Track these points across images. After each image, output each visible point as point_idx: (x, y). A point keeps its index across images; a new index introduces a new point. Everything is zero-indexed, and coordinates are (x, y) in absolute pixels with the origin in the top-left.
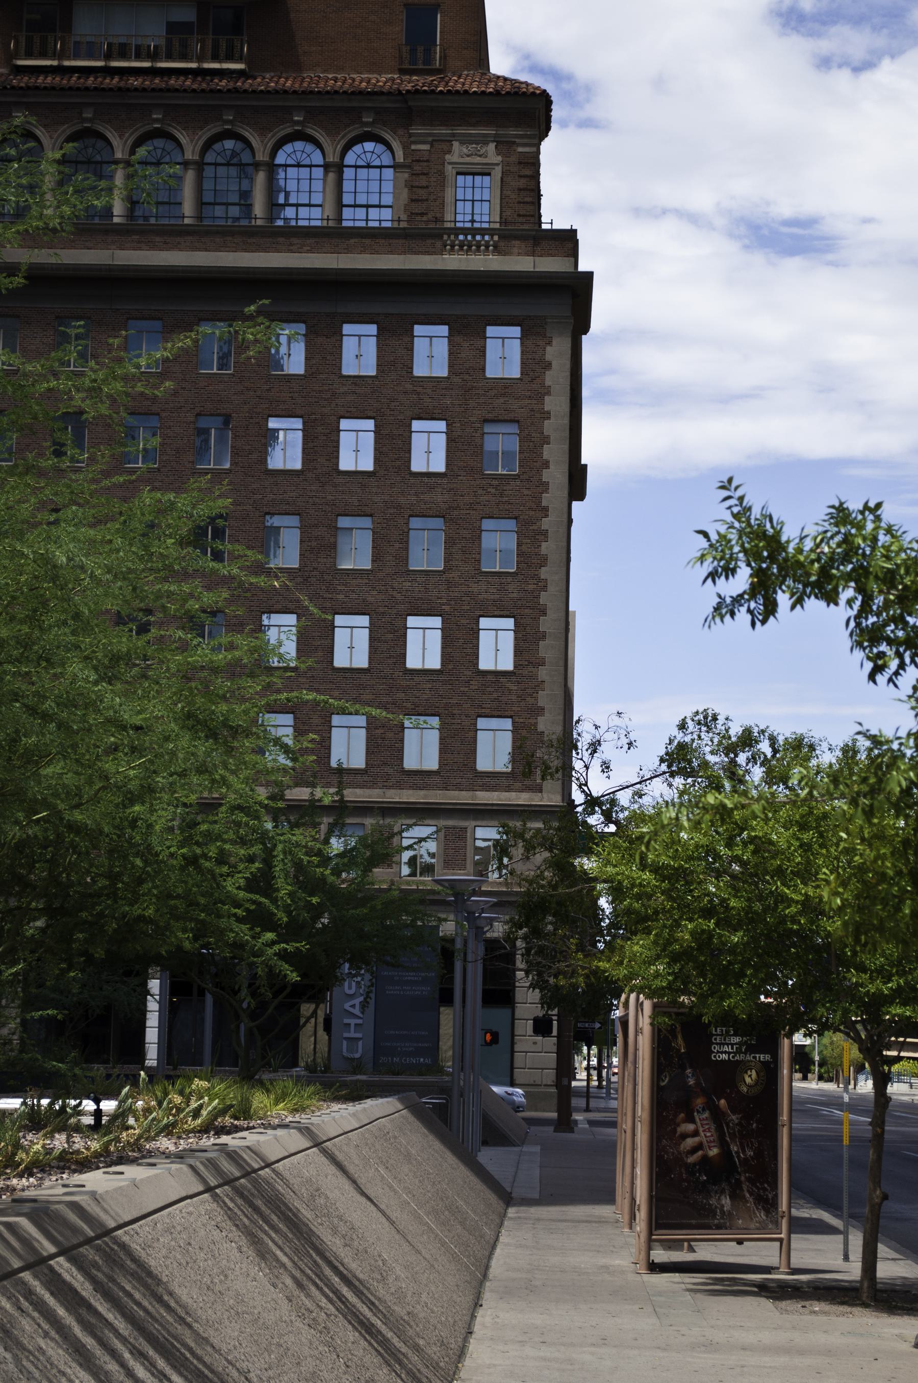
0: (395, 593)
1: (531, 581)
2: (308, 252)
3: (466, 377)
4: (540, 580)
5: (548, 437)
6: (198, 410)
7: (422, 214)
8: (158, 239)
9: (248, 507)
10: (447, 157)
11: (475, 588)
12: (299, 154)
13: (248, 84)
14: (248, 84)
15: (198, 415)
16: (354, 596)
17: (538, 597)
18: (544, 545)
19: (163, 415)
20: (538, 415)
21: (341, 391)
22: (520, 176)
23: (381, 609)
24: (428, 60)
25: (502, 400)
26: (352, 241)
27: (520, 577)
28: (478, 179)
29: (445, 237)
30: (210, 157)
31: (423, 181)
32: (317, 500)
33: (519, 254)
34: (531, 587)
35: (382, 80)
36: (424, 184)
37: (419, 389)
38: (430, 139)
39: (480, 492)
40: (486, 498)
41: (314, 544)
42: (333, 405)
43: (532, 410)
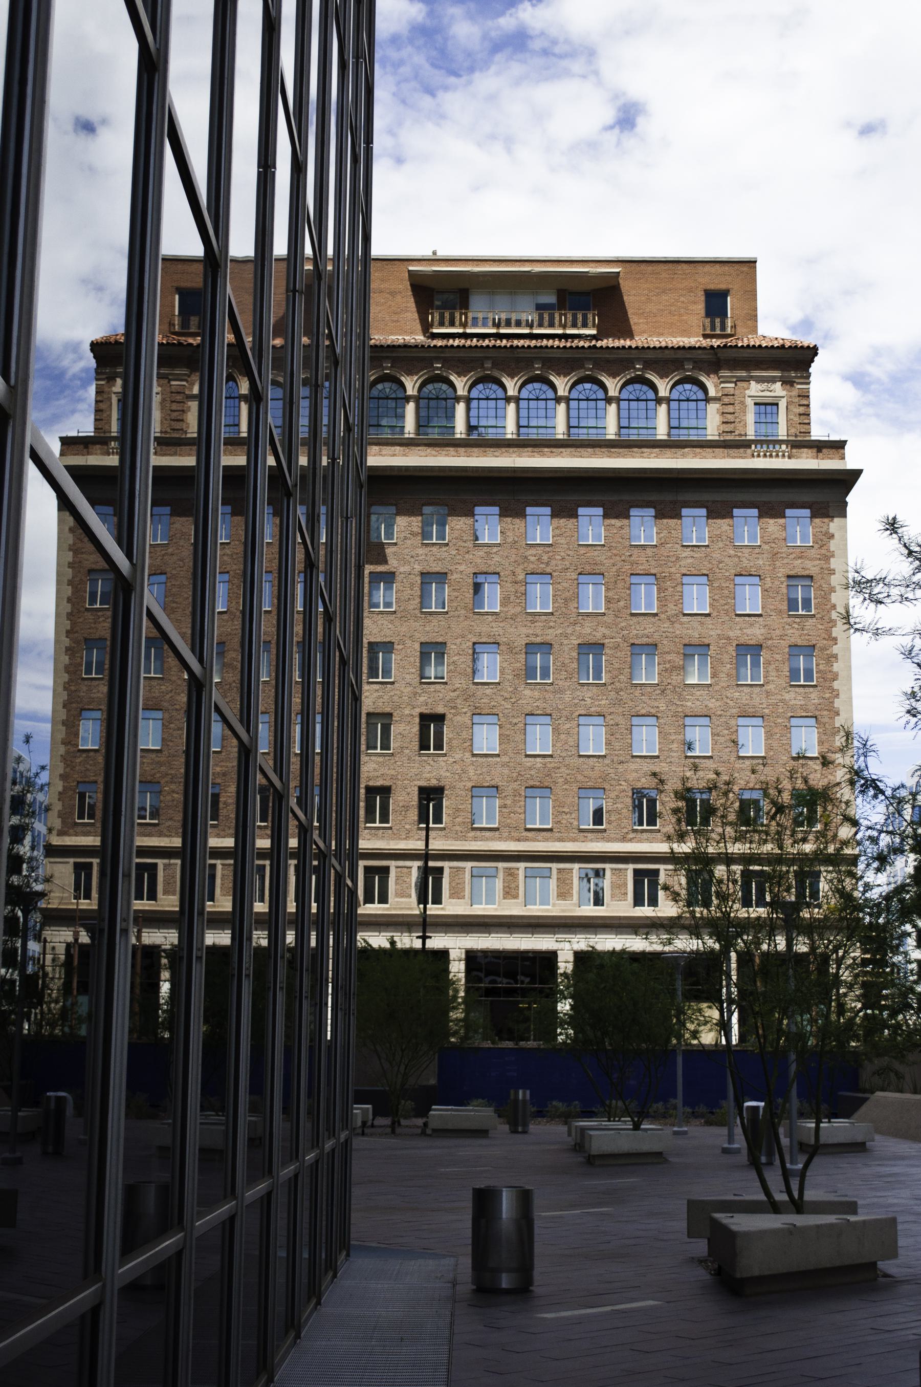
0: (728, 701)
1: (827, 691)
2: (656, 457)
3: (773, 545)
4: (833, 690)
5: (834, 587)
6: (579, 570)
7: (731, 432)
8: (546, 450)
9: (619, 640)
10: (747, 392)
11: (787, 697)
12: (638, 392)
13: (599, 344)
14: (599, 344)
15: (580, 574)
16: (698, 703)
17: (833, 702)
18: (835, 664)
19: (554, 574)
20: (826, 572)
21: (683, 555)
22: (800, 405)
23: (719, 713)
24: (723, 327)
25: (800, 561)
26: (686, 450)
27: (819, 688)
28: (769, 408)
29: (753, 446)
30: (574, 394)
31: (730, 409)
32: (669, 634)
33: (807, 458)
34: (827, 695)
35: (694, 340)
36: (732, 411)
37: (739, 554)
38: (734, 380)
39: (787, 627)
40: (791, 631)
41: (668, 666)
42: (678, 566)
43: (822, 568)
